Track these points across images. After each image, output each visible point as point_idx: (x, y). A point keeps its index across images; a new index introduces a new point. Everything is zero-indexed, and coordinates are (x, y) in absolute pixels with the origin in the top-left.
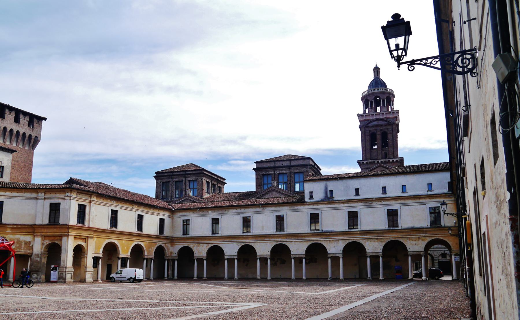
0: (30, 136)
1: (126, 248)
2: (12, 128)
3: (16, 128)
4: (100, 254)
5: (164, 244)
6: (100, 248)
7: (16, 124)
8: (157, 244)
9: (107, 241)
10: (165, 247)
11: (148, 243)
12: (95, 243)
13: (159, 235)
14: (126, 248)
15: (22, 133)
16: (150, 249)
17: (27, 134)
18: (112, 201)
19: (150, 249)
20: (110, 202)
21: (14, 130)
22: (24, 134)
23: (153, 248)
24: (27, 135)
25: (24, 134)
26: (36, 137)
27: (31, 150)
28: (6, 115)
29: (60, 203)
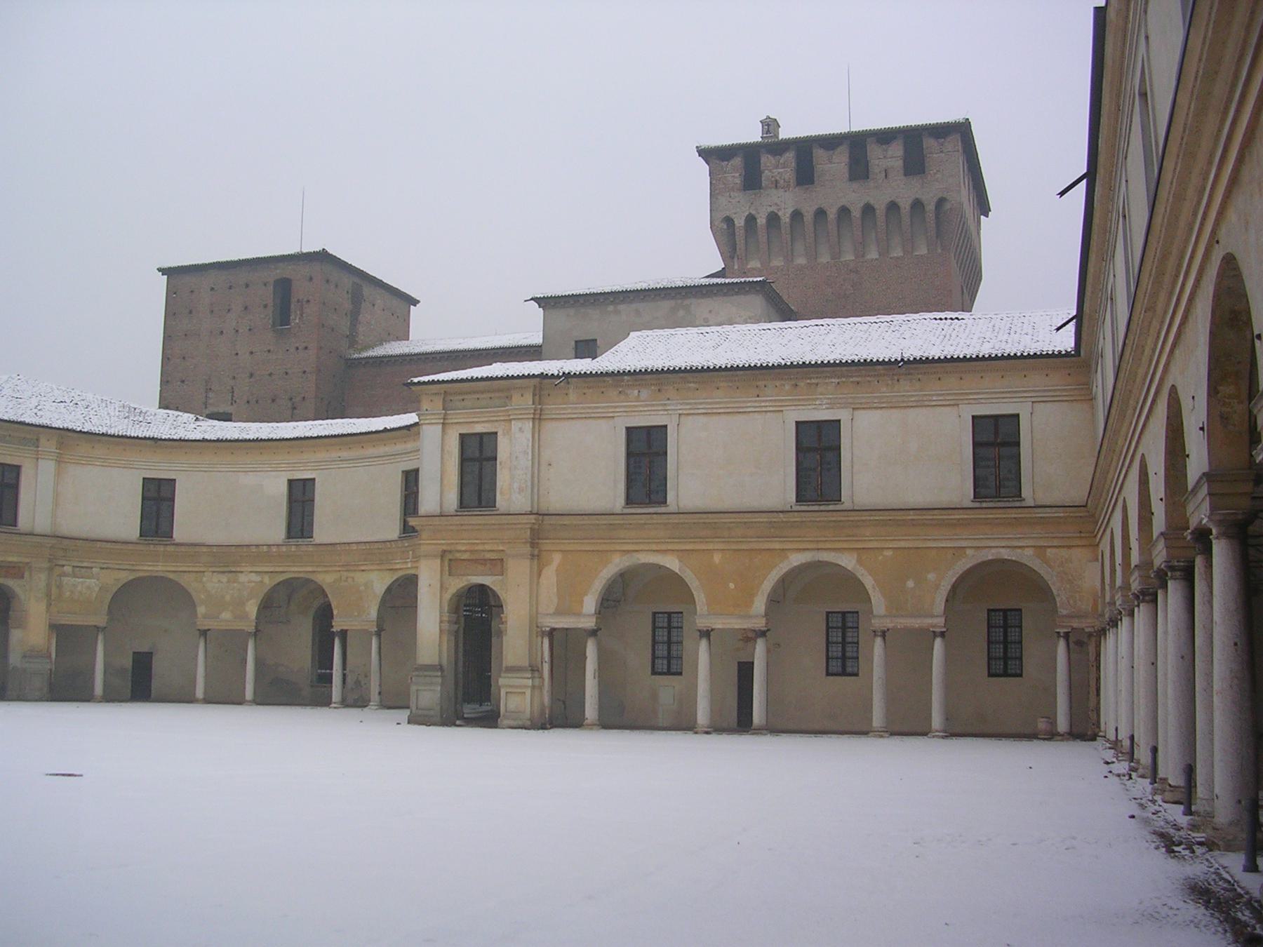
0: (917, 205)
1: (732, 586)
2: (843, 202)
3: (854, 196)
4: (585, 616)
5: (1029, 552)
6: (587, 595)
7: (855, 185)
8: (969, 552)
9: (617, 564)
10: (1036, 564)
11: (889, 553)
12: (557, 576)
13: (977, 505)
14: (732, 586)
15: (883, 207)
16: (910, 584)
17: (901, 204)
18: (629, 392)
19: (910, 584)
20: (622, 397)
21: (852, 209)
22: (893, 207)
23: (931, 576)
24: (905, 205)
25: (893, 207)
26: (941, 202)
27: (940, 251)
28: (819, 168)
29: (17, 469)
